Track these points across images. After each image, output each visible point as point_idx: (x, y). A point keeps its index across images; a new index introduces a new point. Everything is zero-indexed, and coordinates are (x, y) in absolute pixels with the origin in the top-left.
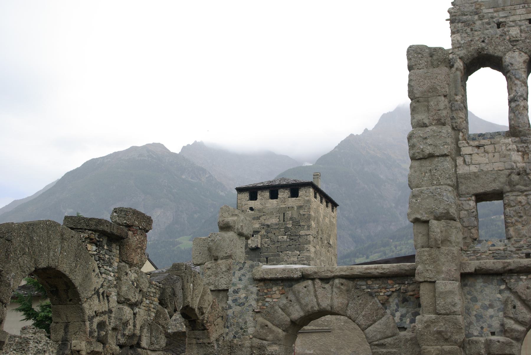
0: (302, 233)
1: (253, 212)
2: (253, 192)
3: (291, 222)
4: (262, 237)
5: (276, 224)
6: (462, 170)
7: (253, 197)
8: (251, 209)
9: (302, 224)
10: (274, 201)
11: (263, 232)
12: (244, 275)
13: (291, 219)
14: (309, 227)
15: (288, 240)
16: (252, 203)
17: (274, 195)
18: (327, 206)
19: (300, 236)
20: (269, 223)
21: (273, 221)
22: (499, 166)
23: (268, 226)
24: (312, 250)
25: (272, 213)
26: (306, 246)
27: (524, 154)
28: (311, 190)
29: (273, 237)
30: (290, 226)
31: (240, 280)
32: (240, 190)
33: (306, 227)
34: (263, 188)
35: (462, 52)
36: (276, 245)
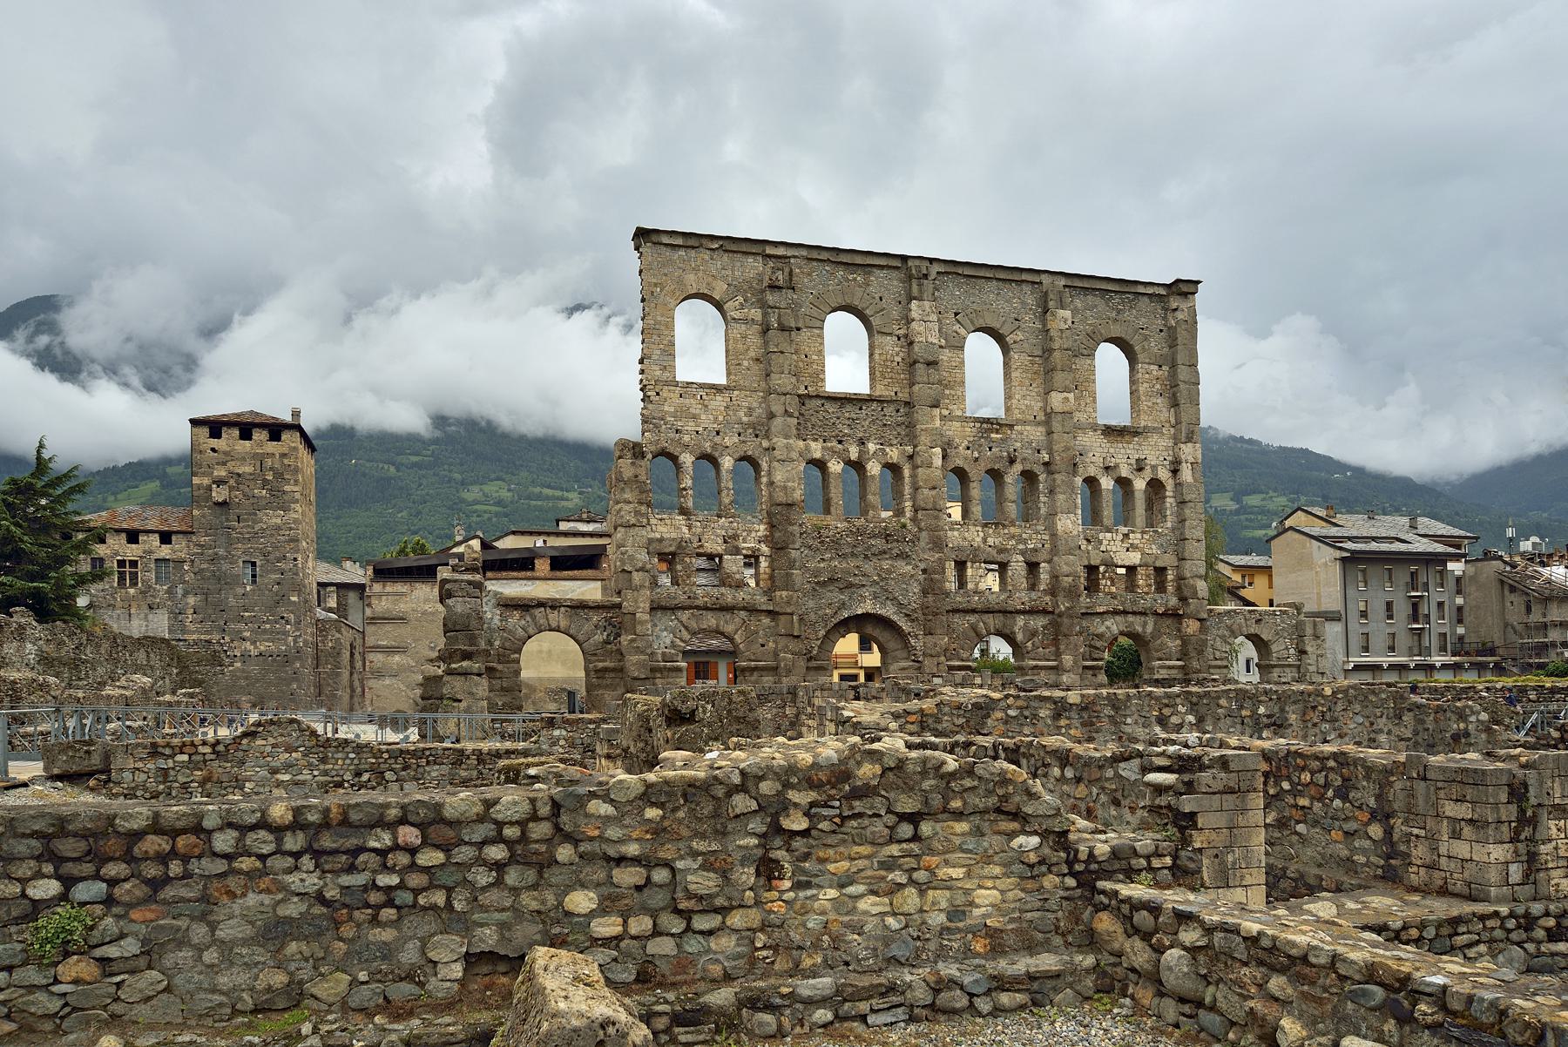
0: (287, 488)
4: (231, 489)
6: (652, 535)
8: (213, 450)
11: (232, 482)
13: (271, 469)
14: (296, 481)
16: (214, 443)
19: (284, 492)
21: (248, 469)
22: (673, 535)
25: (244, 459)
27: (690, 527)
34: (230, 424)
35: (653, 448)
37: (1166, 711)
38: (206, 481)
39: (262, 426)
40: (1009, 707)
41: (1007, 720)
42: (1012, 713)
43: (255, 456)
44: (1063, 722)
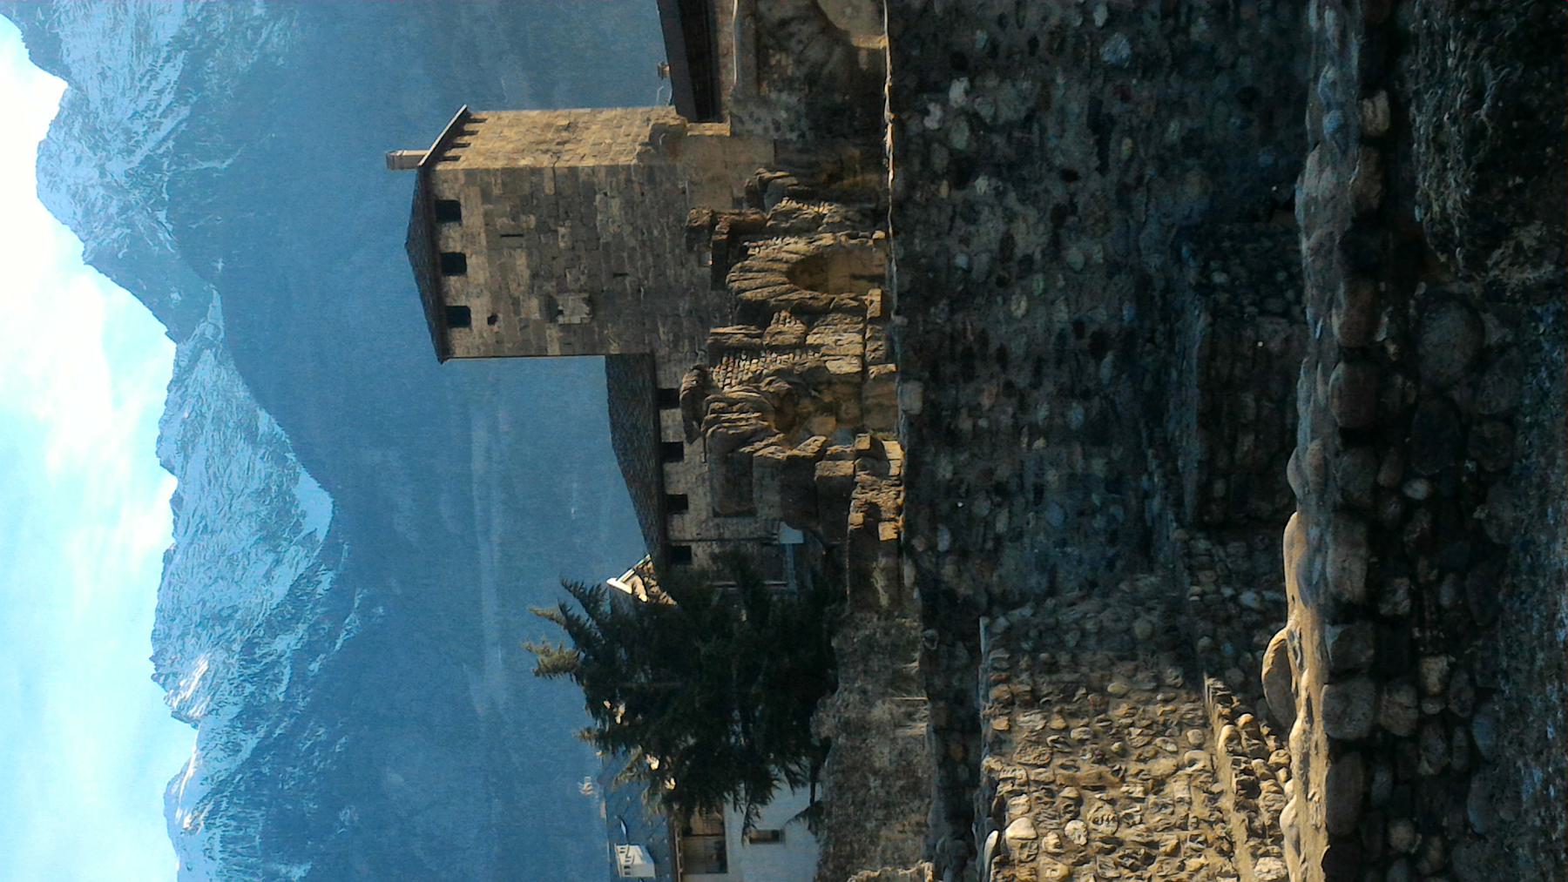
0: (549, 188)
1: (500, 316)
2: (447, 319)
3: (523, 218)
4: (563, 289)
5: (530, 255)
7: (461, 317)
8: (492, 320)
9: (527, 188)
10: (472, 262)
11: (549, 287)
12: (751, 115)
15: (568, 223)
16: (478, 318)
17: (456, 264)
18: (472, 133)
19: (558, 193)
20: (526, 274)
21: (521, 262)
23: (534, 276)
24: (590, 162)
26: (582, 177)
28: (440, 167)
29: (562, 261)
30: (532, 218)
31: (758, 120)
32: (444, 351)
33: (534, 179)
36: (582, 253)
37: (940, 160)
38: (553, 333)
39: (432, 237)
40: (932, 547)
41: (962, 553)
42: (944, 542)
43: (494, 249)
44: (965, 424)
